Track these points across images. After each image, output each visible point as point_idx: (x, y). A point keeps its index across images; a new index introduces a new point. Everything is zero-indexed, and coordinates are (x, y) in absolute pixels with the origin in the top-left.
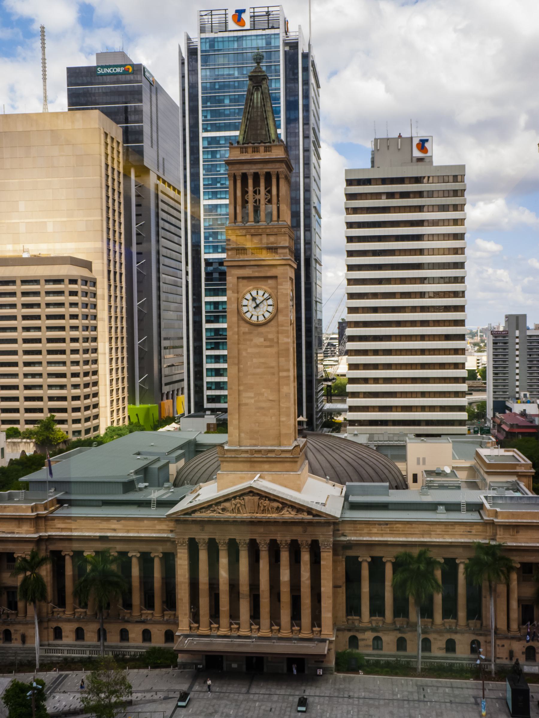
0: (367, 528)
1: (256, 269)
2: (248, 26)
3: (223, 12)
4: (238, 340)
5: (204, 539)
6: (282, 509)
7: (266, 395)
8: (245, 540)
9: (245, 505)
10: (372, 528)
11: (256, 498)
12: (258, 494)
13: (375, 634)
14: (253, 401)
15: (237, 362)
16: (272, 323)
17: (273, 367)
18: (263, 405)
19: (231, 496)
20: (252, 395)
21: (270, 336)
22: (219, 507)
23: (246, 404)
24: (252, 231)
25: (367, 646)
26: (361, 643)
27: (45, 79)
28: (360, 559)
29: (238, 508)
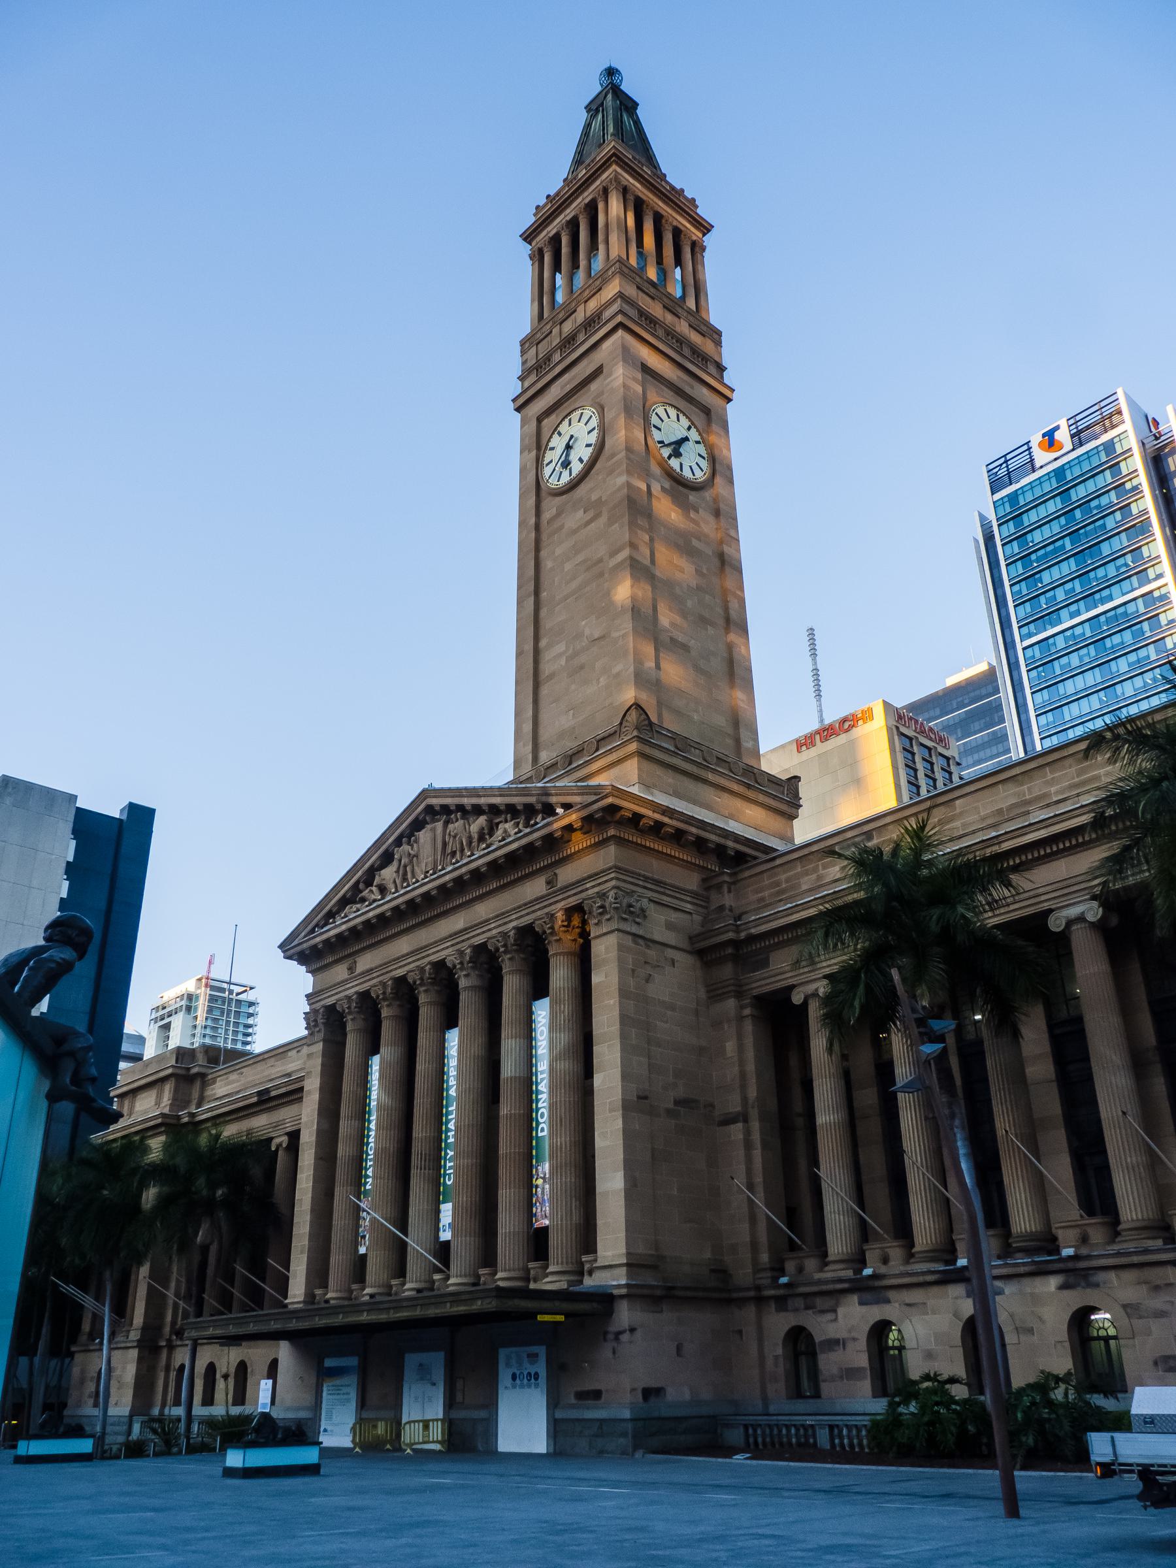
0: (807, 873)
1: (566, 377)
2: (1068, 446)
3: (1025, 447)
4: (538, 542)
5: (349, 998)
6: (492, 828)
7: (587, 632)
8: (422, 969)
9: (416, 856)
10: (824, 868)
11: (439, 825)
12: (446, 809)
13: (876, 1313)
14: (563, 662)
15: (532, 588)
16: (598, 466)
17: (600, 560)
18: (583, 659)
19: (390, 840)
20: (561, 648)
21: (594, 497)
22: (374, 889)
23: (552, 676)
24: (561, 315)
25: (851, 1373)
26: (829, 1362)
27: (819, 696)
28: (797, 998)
29: (405, 866)
